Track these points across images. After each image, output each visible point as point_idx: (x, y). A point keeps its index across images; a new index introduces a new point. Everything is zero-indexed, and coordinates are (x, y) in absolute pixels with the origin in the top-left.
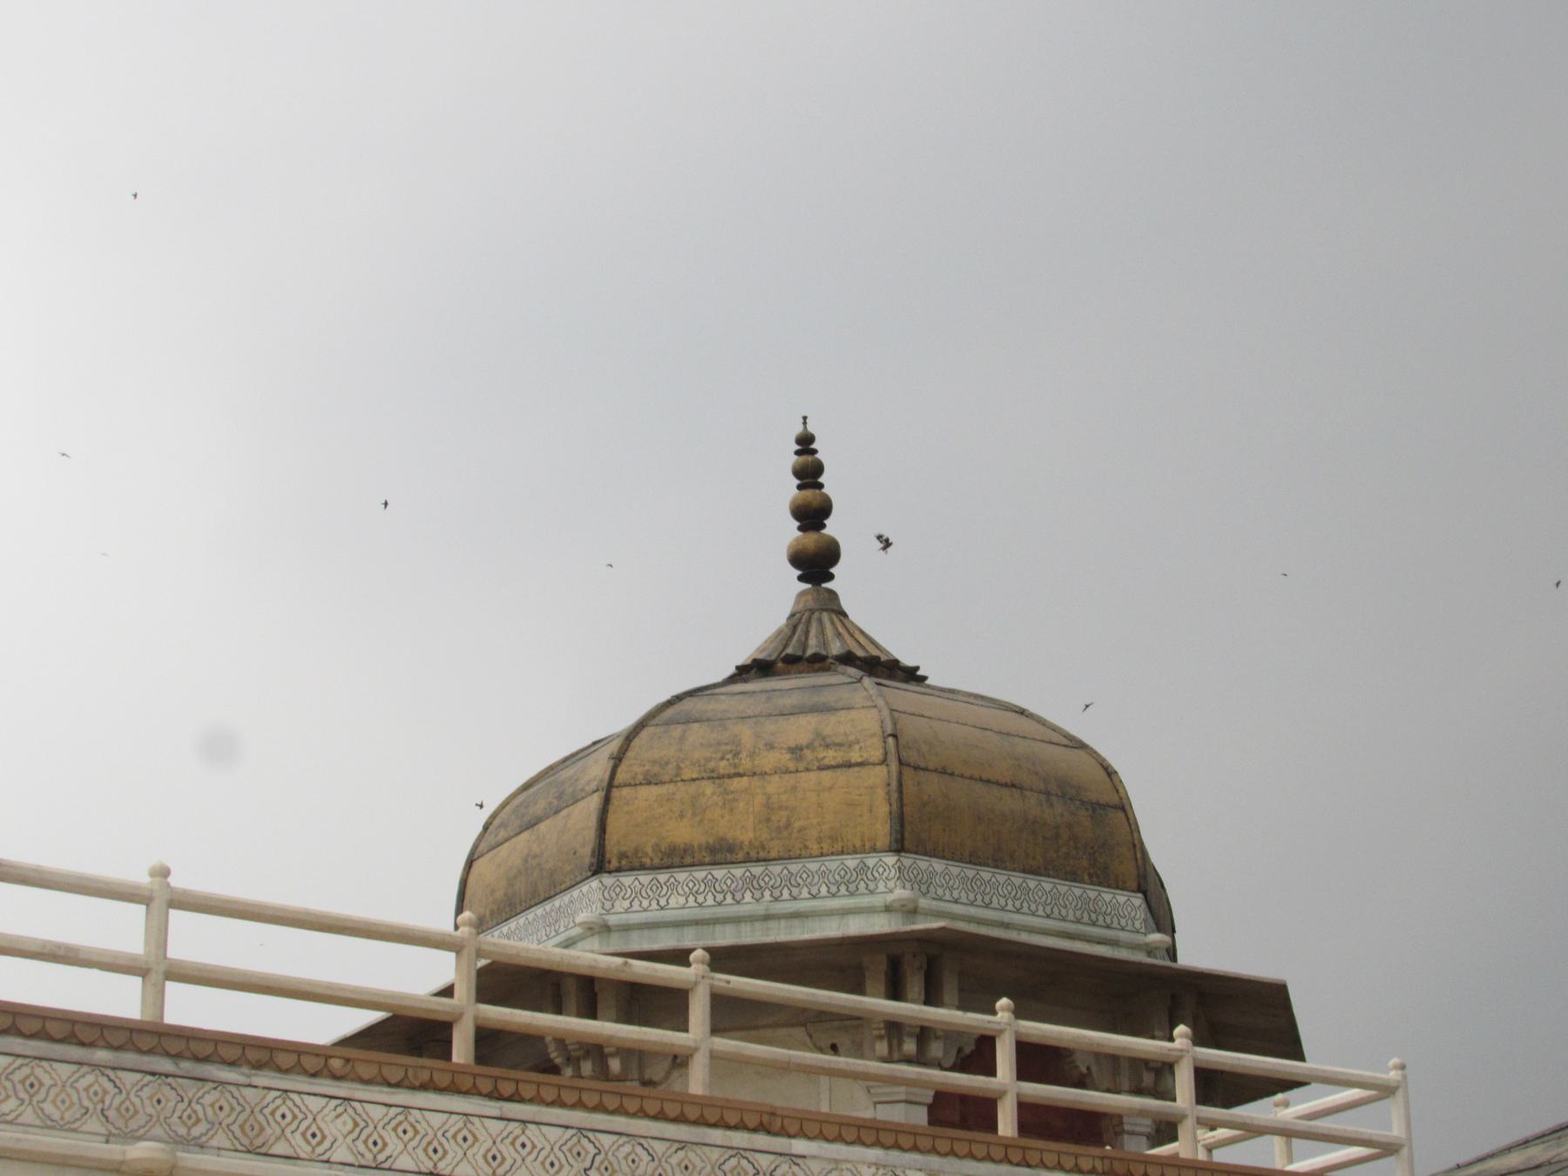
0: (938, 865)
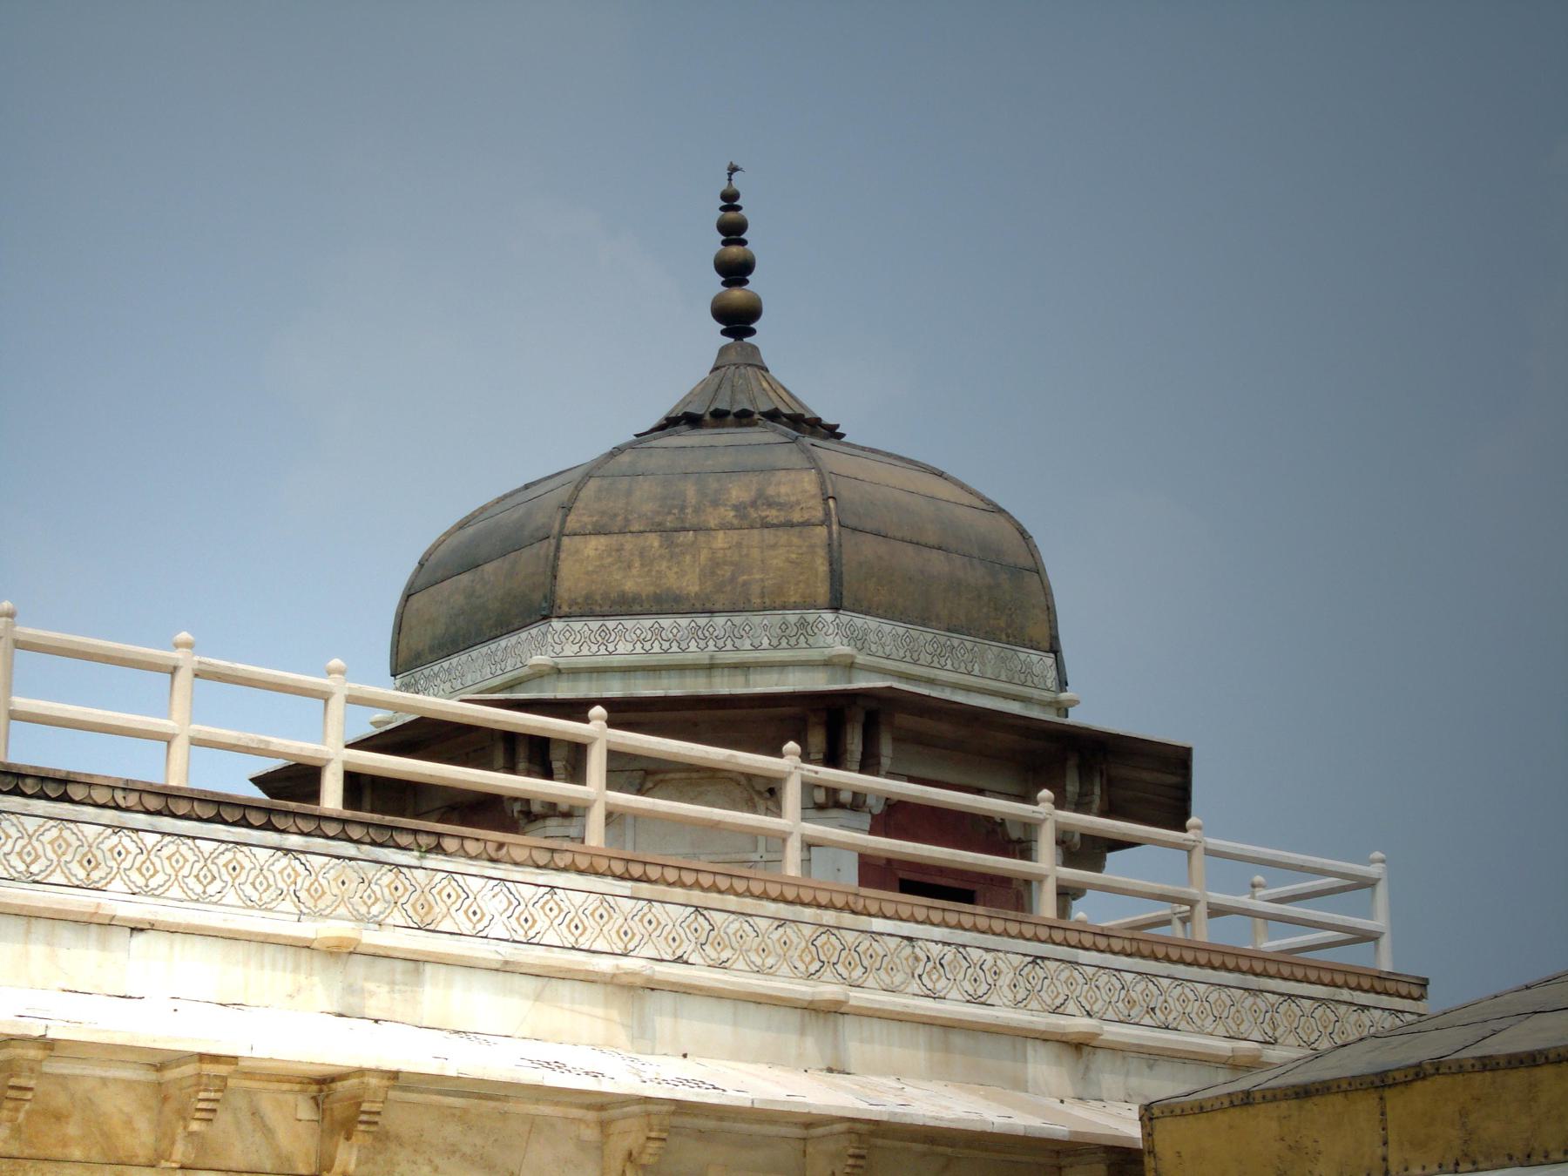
0: (872, 623)
